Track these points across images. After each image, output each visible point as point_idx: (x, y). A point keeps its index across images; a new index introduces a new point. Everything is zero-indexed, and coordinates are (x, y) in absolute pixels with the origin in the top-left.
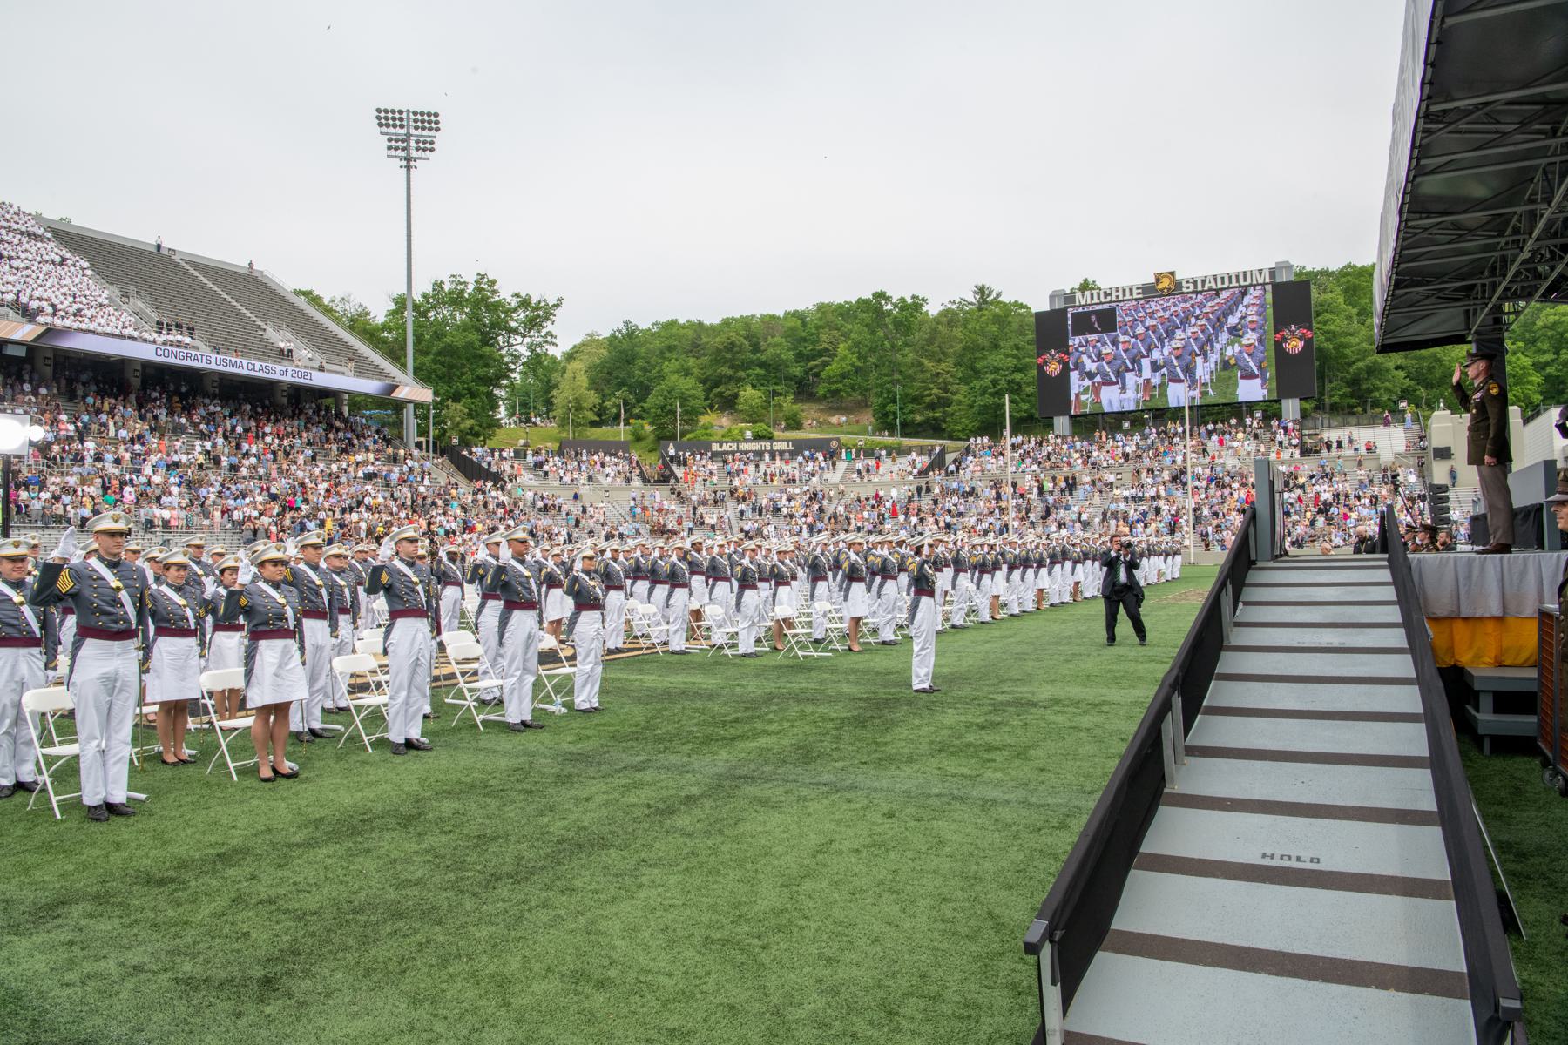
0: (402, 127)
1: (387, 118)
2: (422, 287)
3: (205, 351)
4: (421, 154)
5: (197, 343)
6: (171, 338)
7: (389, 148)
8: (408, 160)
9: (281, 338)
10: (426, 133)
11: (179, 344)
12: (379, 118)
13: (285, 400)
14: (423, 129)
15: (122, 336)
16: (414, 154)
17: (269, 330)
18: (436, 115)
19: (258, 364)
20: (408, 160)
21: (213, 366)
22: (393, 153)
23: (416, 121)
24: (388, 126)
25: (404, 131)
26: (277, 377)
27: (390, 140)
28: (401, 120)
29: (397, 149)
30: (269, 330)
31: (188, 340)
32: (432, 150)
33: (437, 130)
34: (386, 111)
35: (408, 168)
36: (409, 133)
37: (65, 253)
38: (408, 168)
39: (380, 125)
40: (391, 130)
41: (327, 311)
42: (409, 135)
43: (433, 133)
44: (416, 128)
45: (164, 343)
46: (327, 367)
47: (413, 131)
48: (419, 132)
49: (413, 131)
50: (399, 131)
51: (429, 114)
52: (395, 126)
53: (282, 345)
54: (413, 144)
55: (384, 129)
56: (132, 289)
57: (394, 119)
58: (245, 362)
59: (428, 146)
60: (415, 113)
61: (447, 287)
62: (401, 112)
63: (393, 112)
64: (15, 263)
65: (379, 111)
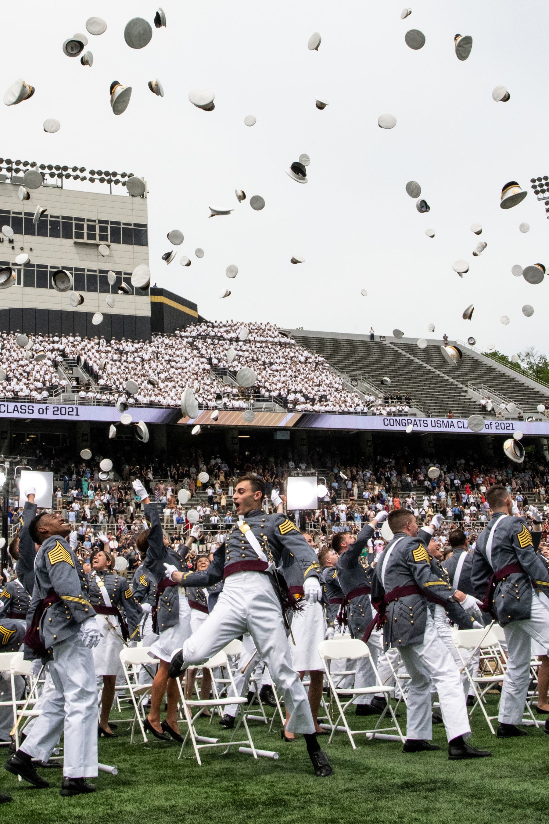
3: (421, 416)
5: (414, 410)
6: (393, 409)
9: (482, 396)
11: (401, 413)
13: (491, 452)
15: (356, 413)
17: (470, 390)
19: (466, 422)
21: (430, 429)
24: (543, 191)
26: (484, 431)
30: (470, 390)
31: (407, 409)
34: (540, 179)
37: (306, 354)
39: (537, 192)
41: (515, 366)
45: (389, 414)
46: (525, 416)
53: (483, 402)
55: (541, 195)
56: (358, 373)
58: (455, 421)
64: (274, 367)
65: (533, 181)
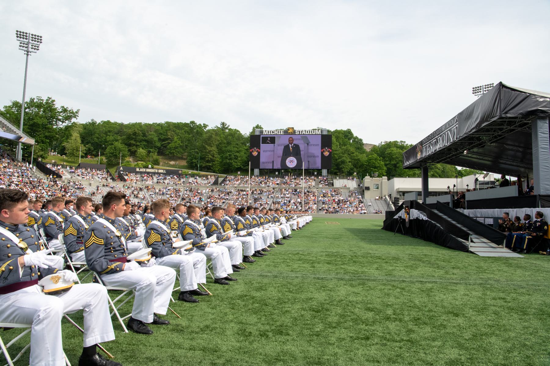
0: (26, 39)
1: (20, 35)
2: (27, 100)
4: (33, 50)
7: (20, 46)
8: (28, 52)
10: (36, 43)
12: (17, 34)
14: (35, 41)
16: (30, 50)
18: (41, 37)
20: (28, 52)
22: (22, 48)
23: (32, 38)
24: (21, 38)
25: (27, 41)
27: (21, 43)
28: (26, 36)
29: (23, 47)
32: (38, 50)
33: (41, 42)
35: (28, 55)
36: (29, 42)
38: (28, 55)
39: (18, 37)
40: (22, 39)
42: (28, 43)
43: (38, 43)
44: (32, 40)
47: (31, 41)
48: (33, 42)
49: (31, 41)
50: (25, 40)
51: (38, 36)
52: (23, 38)
54: (30, 46)
55: (19, 39)
57: (23, 35)
59: (37, 48)
60: (32, 35)
61: (35, 101)
62: (26, 33)
63: (23, 33)
65: (17, 31)
